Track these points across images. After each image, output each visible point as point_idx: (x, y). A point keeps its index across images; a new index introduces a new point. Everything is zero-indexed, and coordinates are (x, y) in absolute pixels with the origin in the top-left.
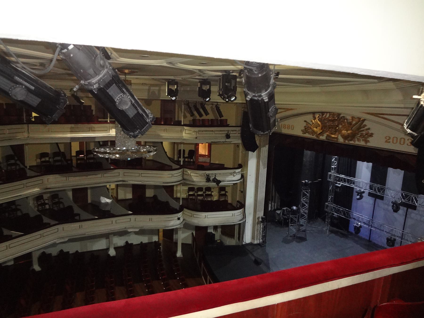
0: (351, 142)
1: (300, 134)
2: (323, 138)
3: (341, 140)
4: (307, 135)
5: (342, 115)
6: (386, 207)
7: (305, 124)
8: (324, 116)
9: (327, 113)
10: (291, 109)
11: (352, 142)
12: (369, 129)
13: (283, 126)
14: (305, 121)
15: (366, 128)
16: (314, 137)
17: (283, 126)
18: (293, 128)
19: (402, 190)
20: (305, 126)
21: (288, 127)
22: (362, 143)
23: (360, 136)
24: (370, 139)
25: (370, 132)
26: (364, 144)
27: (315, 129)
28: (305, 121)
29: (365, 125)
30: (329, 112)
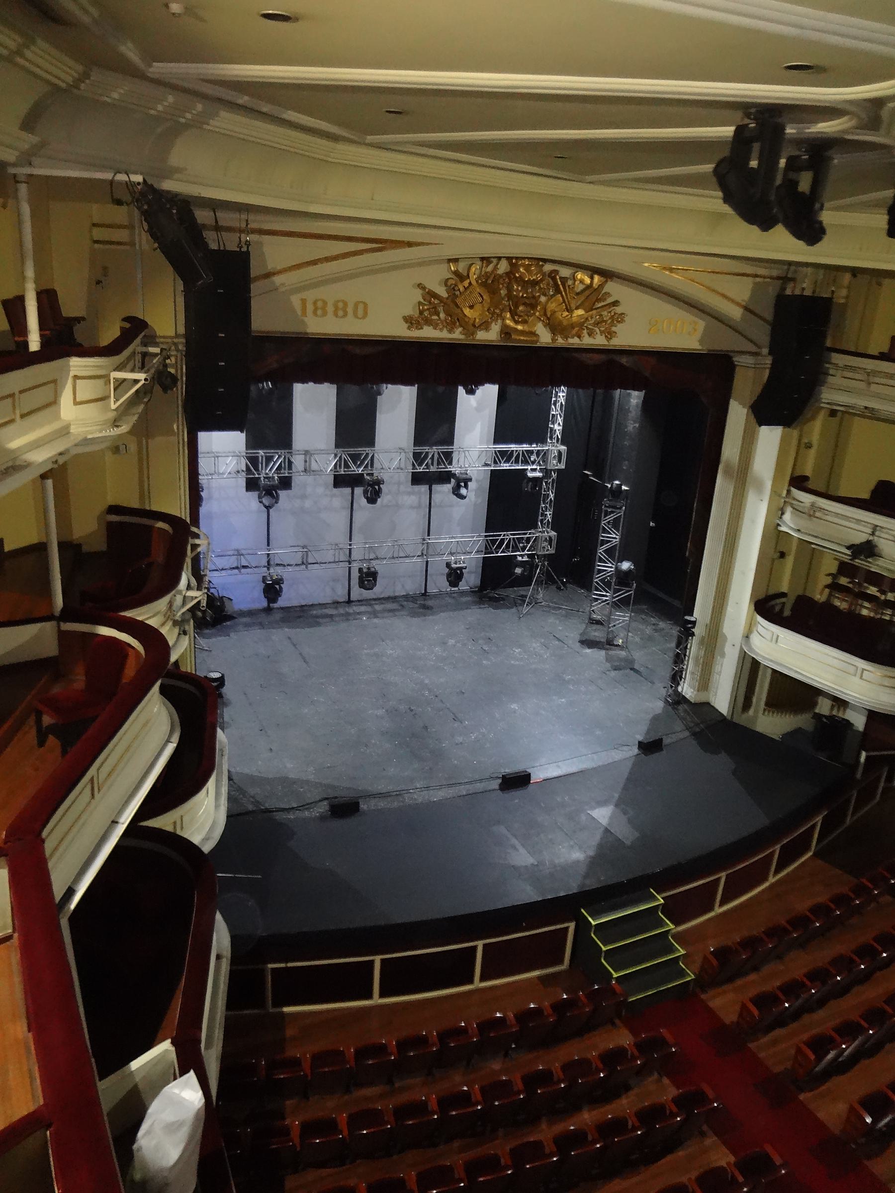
0: (571, 341)
1: (399, 330)
2: (491, 335)
3: (545, 337)
4: (428, 333)
5: (548, 267)
6: (297, 503)
7: (418, 295)
8: (490, 268)
9: (499, 258)
10: (410, 244)
11: (576, 340)
12: (616, 303)
13: (310, 307)
14: (420, 286)
15: (609, 300)
16: (457, 335)
17: (310, 307)
18: (362, 310)
19: (337, 446)
20: (420, 303)
21: (341, 309)
22: (599, 341)
23: (597, 324)
24: (618, 328)
25: (618, 310)
26: (606, 343)
27: (467, 311)
28: (420, 286)
29: (608, 294)
30: (509, 259)
